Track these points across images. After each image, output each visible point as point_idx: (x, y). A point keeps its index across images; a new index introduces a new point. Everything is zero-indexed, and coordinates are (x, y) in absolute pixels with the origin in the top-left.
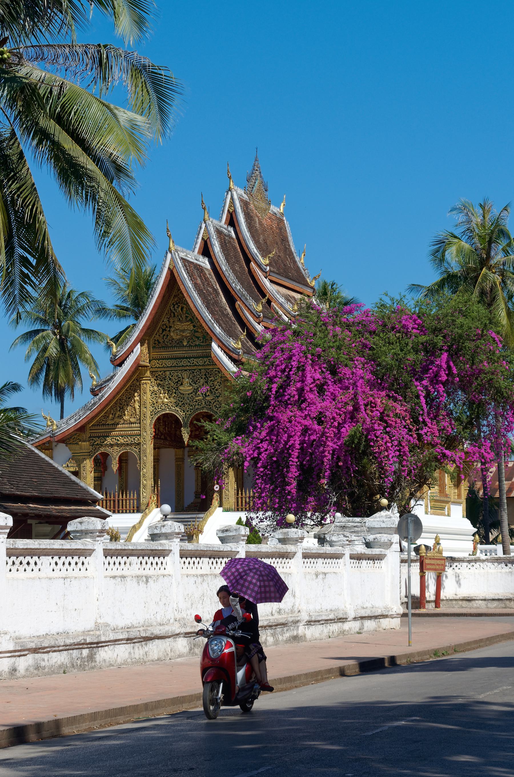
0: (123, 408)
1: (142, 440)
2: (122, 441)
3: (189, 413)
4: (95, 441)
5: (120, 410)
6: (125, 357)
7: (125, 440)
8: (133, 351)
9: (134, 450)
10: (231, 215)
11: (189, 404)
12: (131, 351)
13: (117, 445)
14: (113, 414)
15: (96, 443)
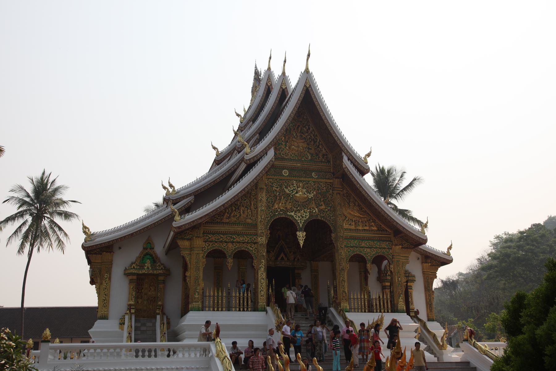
0: (238, 209)
1: (259, 239)
2: (238, 240)
3: (304, 219)
4: (209, 238)
5: (235, 210)
6: (259, 156)
7: (241, 239)
8: (266, 154)
9: (251, 248)
10: (269, 87)
11: (304, 211)
12: (264, 152)
13: (232, 242)
14: (228, 213)
15: (211, 240)
